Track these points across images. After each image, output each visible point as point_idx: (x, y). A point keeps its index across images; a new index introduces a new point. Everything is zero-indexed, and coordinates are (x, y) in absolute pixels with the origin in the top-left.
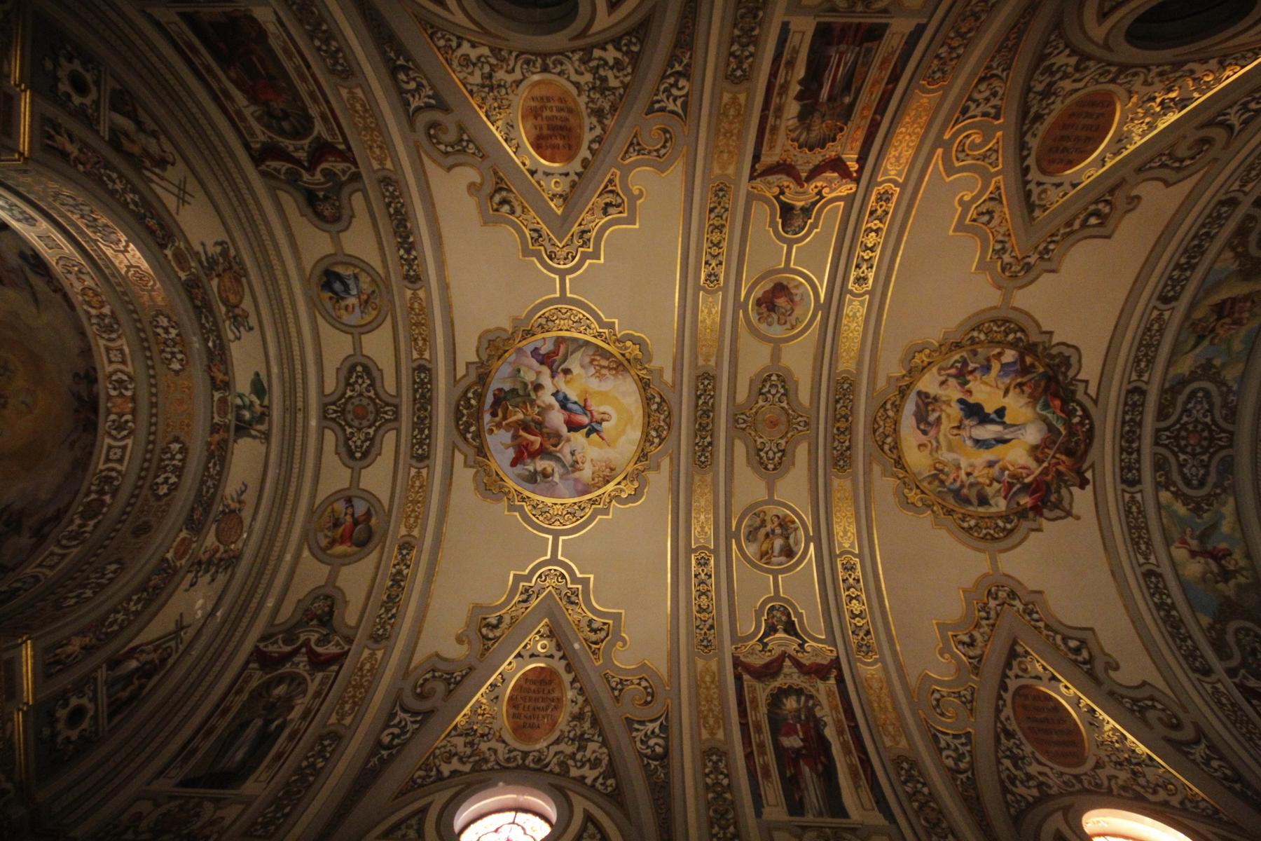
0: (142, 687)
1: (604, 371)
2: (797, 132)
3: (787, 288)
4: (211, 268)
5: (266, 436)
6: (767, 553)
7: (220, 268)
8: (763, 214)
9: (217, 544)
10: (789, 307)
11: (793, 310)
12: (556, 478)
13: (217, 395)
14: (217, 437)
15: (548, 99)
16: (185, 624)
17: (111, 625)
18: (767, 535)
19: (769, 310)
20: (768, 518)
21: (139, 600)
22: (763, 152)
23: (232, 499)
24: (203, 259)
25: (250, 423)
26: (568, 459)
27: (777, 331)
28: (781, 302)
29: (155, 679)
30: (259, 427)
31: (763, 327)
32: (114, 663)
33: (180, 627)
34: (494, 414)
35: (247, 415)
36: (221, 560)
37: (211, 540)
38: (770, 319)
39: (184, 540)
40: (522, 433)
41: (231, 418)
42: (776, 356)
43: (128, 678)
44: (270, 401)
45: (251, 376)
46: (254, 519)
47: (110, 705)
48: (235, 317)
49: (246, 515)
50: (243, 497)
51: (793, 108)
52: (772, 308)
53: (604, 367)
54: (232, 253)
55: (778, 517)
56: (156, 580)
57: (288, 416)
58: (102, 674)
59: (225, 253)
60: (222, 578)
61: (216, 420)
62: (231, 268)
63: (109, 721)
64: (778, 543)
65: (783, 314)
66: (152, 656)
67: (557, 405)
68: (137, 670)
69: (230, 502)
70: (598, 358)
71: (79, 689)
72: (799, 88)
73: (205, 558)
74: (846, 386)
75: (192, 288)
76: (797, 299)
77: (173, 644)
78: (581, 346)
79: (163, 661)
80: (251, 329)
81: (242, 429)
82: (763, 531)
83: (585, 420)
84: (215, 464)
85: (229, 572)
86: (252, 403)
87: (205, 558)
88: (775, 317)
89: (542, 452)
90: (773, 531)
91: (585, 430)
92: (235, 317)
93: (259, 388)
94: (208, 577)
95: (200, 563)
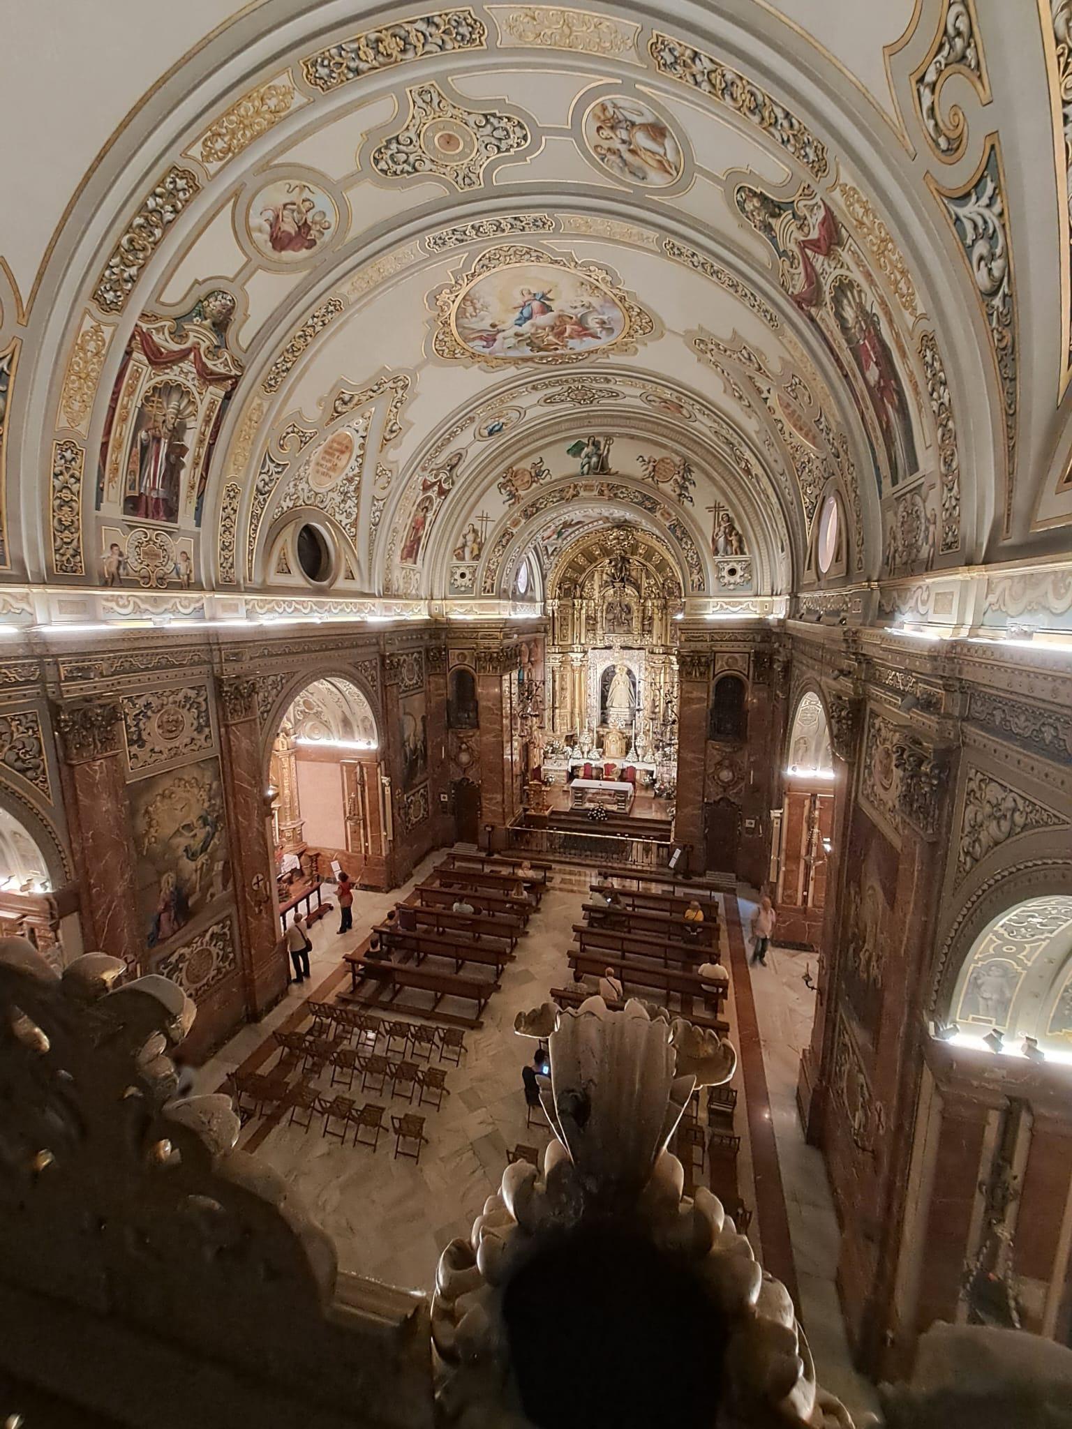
0: (737, 534)
1: (478, 306)
2: (187, 412)
3: (272, 236)
4: (514, 496)
5: (609, 437)
6: (660, 162)
7: (513, 489)
8: (243, 333)
9: (671, 482)
10: (285, 212)
11: (285, 206)
12: (605, 318)
13: (582, 493)
14: (606, 492)
15: (323, 474)
16: (713, 505)
17: (692, 559)
18: (633, 152)
19: (310, 228)
20: (606, 144)
21: (686, 543)
22: (220, 400)
23: (647, 469)
24: (511, 502)
25: (599, 456)
26: (583, 311)
27: (322, 201)
28: (289, 227)
29: (737, 526)
30: (602, 447)
31: (332, 218)
32: (716, 552)
33: (717, 508)
34: (557, 349)
35: (594, 459)
36: (683, 477)
37: (667, 487)
38: (317, 218)
39: (662, 515)
40: (566, 335)
41: (595, 481)
42: (352, 180)
43: (728, 542)
44: (584, 436)
45: (570, 456)
46: (664, 446)
47: (736, 554)
48: (537, 475)
49: (658, 454)
50: (647, 459)
51: (190, 439)
52: (304, 227)
53: (475, 309)
54: (501, 480)
55: (599, 128)
56: (679, 533)
57: (594, 421)
58: (718, 558)
59: (502, 486)
60: (696, 475)
61: (596, 493)
62: (510, 480)
63: (744, 554)
64: (641, 139)
65: (300, 212)
66: (722, 529)
67: (529, 322)
68: (726, 538)
69: (647, 472)
70: (468, 315)
71: (719, 570)
72: (184, 460)
73: (678, 491)
74: (323, 72)
75: (528, 515)
76: (270, 215)
77: (721, 513)
78: (464, 328)
79: (729, 519)
80: (541, 461)
81: (602, 468)
82: (627, 155)
83: (536, 305)
84: (622, 493)
85: (693, 469)
86: (587, 456)
87: (678, 491)
88: (310, 216)
89: (581, 322)
90: (624, 142)
91: (547, 302)
92: (537, 475)
93: (576, 450)
94: (691, 488)
95: (680, 495)
